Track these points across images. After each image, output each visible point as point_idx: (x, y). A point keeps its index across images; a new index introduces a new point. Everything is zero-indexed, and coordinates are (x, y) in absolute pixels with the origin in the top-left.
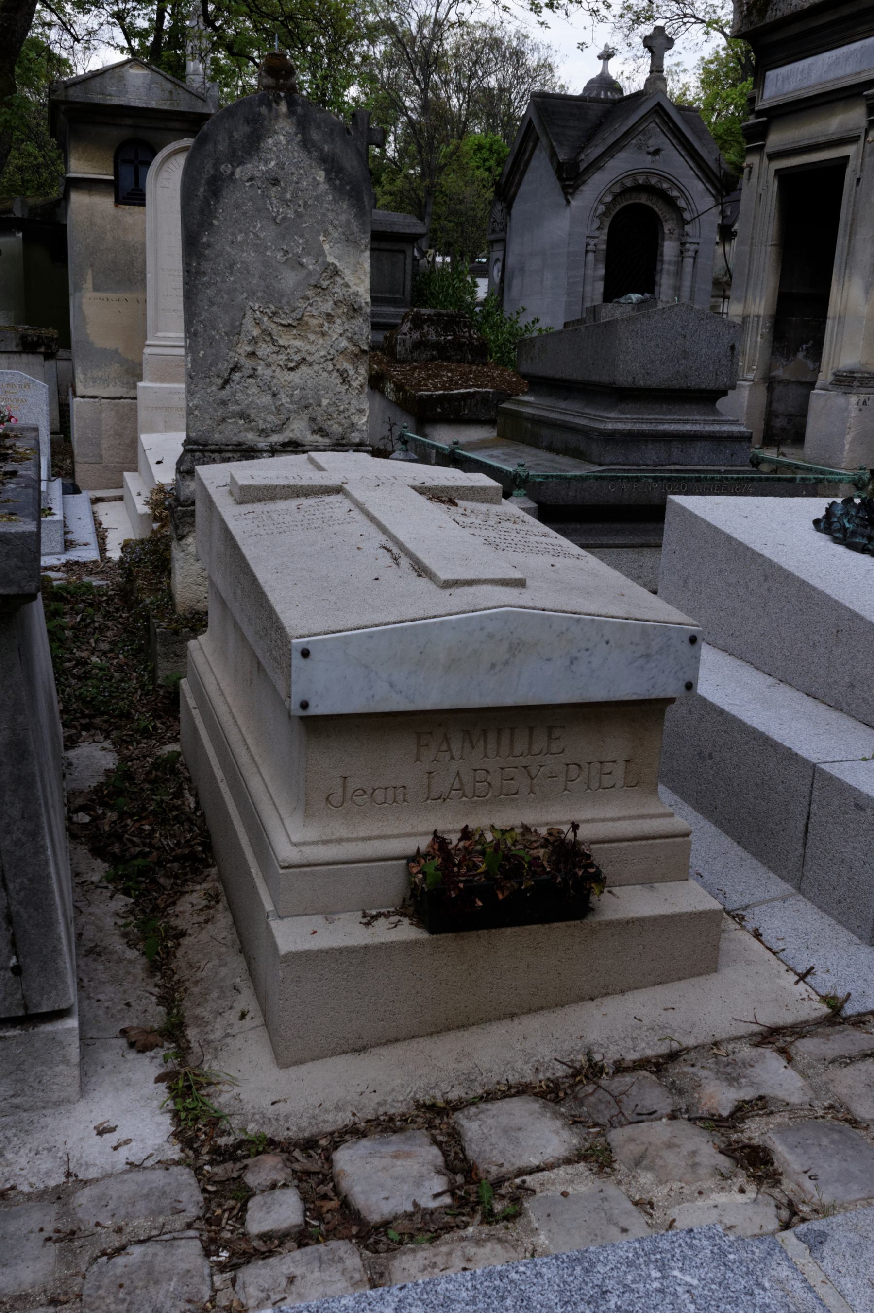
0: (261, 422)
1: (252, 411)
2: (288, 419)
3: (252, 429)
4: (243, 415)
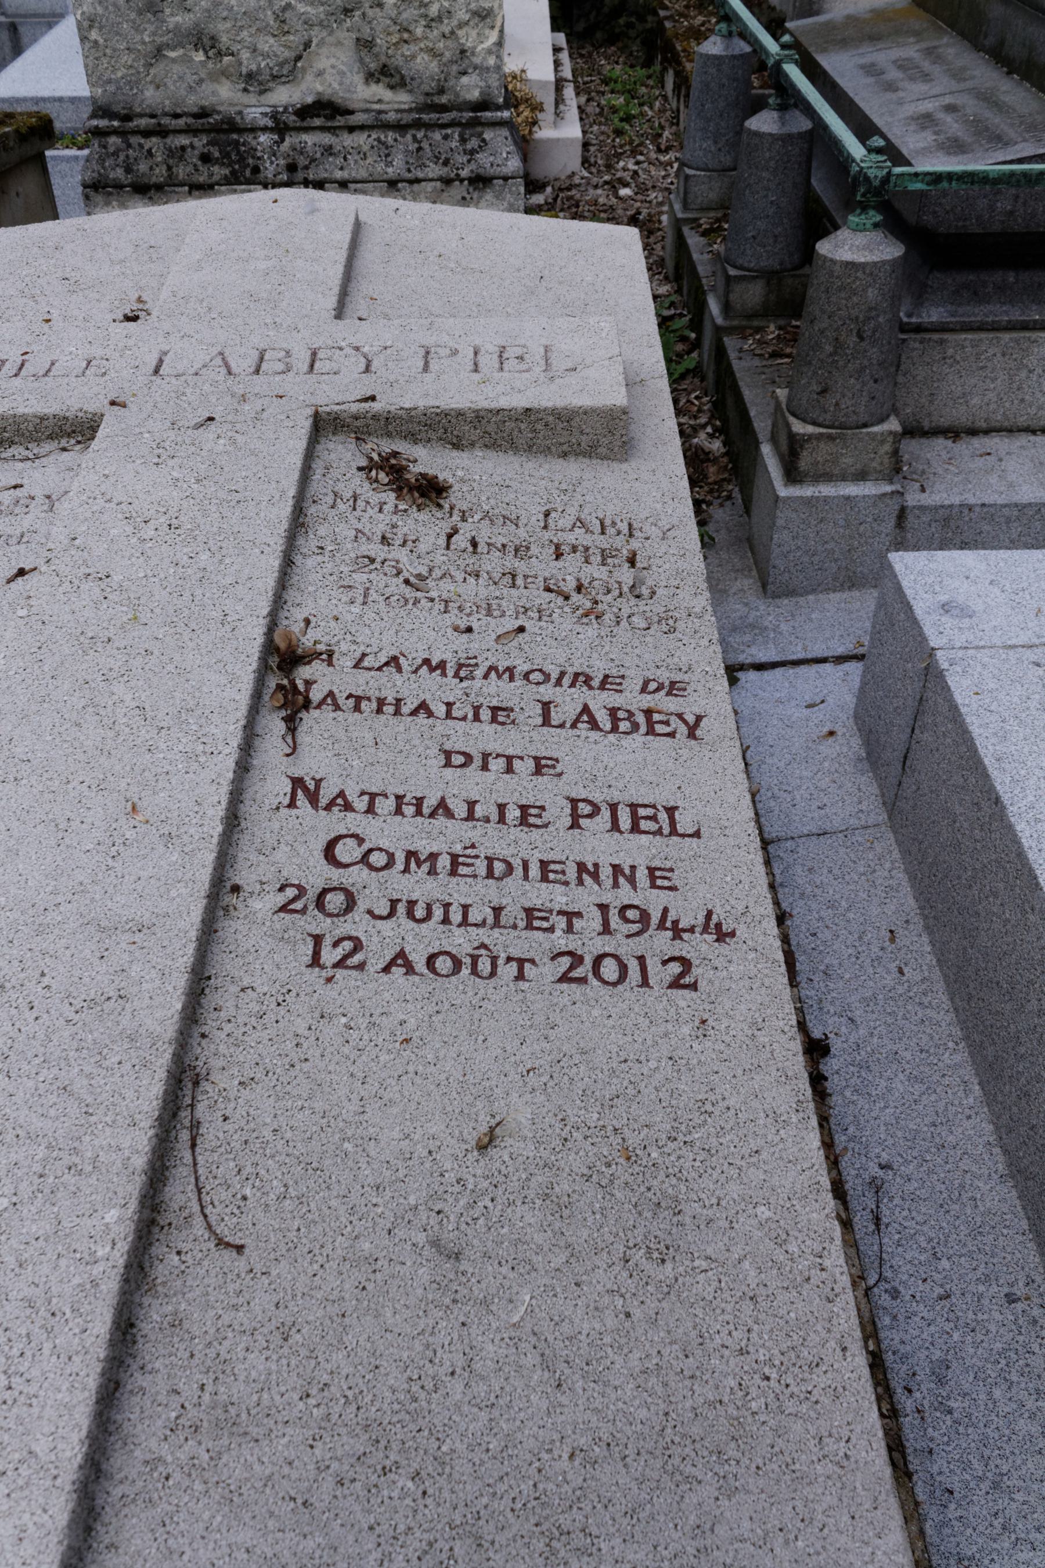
0: (245, 55)
1: (222, 26)
2: (307, 45)
3: (225, 73)
4: (203, 40)
